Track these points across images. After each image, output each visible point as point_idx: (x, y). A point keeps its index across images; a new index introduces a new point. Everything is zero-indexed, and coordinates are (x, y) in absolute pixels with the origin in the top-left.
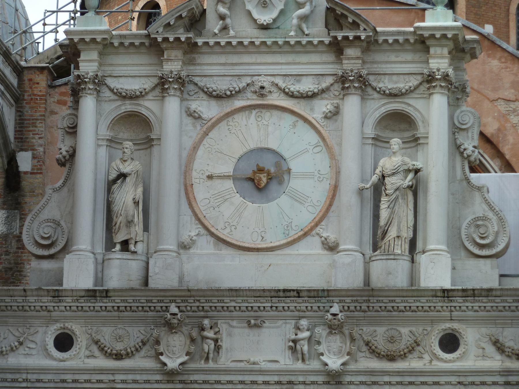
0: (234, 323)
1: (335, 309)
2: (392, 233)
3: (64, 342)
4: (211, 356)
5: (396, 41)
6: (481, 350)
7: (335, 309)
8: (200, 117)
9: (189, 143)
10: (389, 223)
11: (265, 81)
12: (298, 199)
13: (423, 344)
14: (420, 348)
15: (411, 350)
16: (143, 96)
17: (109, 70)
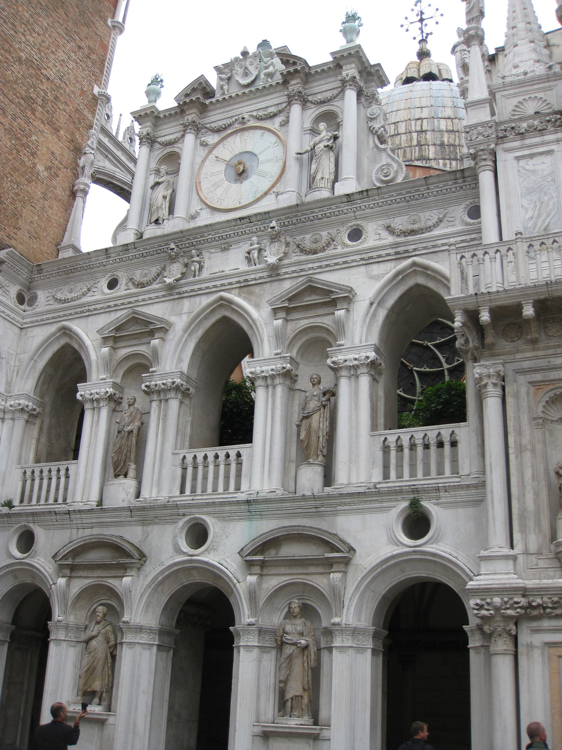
0: (213, 250)
1: (274, 224)
2: (319, 177)
3: (112, 284)
4: (197, 273)
5: (323, 70)
6: (378, 236)
7: (274, 224)
8: (207, 145)
9: (199, 160)
10: (316, 172)
11: (246, 116)
12: (262, 175)
13: (336, 240)
14: (335, 243)
15: (328, 245)
16: (176, 142)
17: (159, 133)
